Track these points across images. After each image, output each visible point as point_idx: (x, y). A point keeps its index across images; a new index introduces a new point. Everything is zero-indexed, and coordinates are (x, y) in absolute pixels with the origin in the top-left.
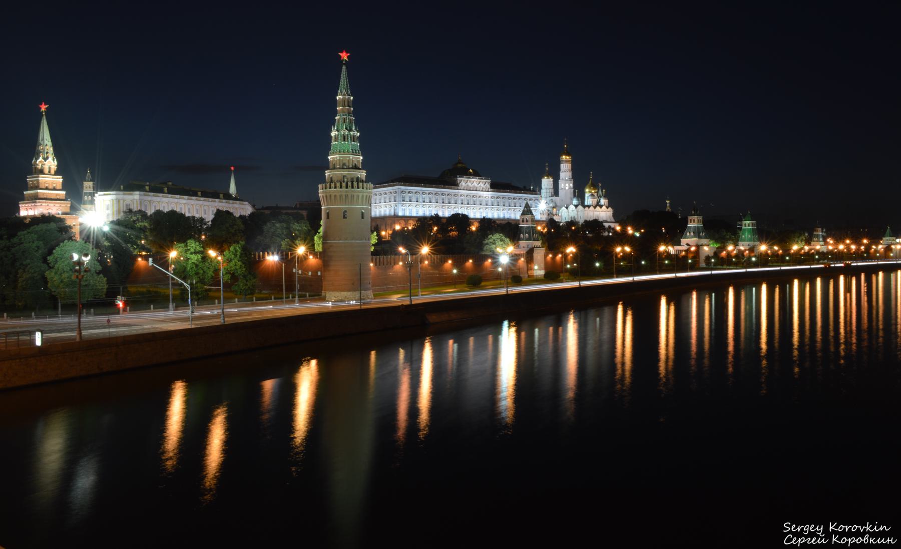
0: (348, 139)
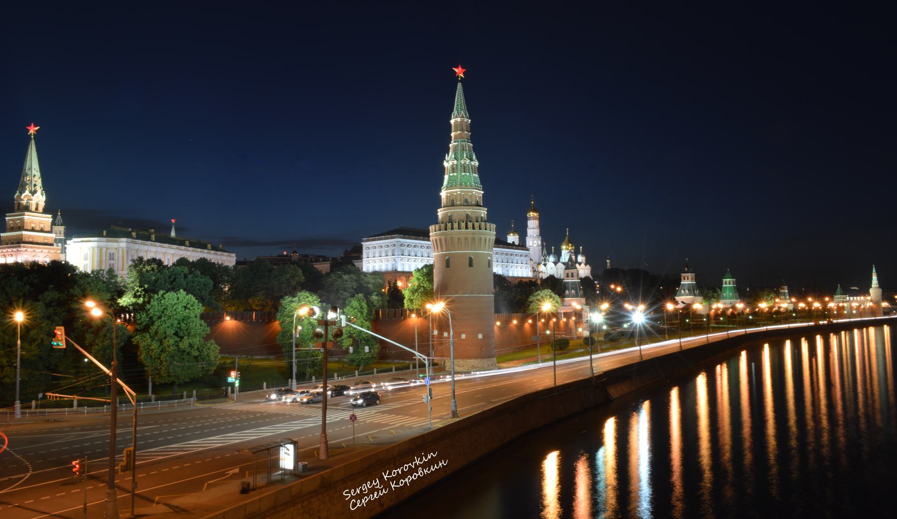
0: (469, 170)
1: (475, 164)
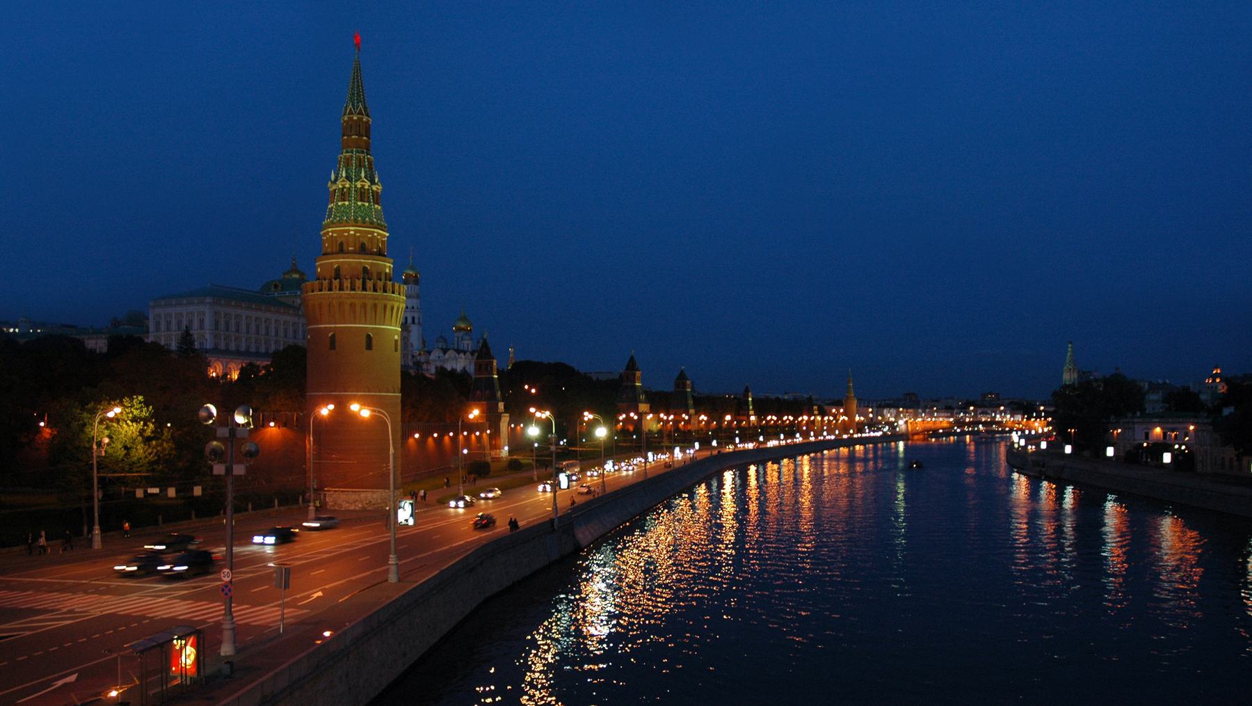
0: (369, 197)
1: (378, 189)
